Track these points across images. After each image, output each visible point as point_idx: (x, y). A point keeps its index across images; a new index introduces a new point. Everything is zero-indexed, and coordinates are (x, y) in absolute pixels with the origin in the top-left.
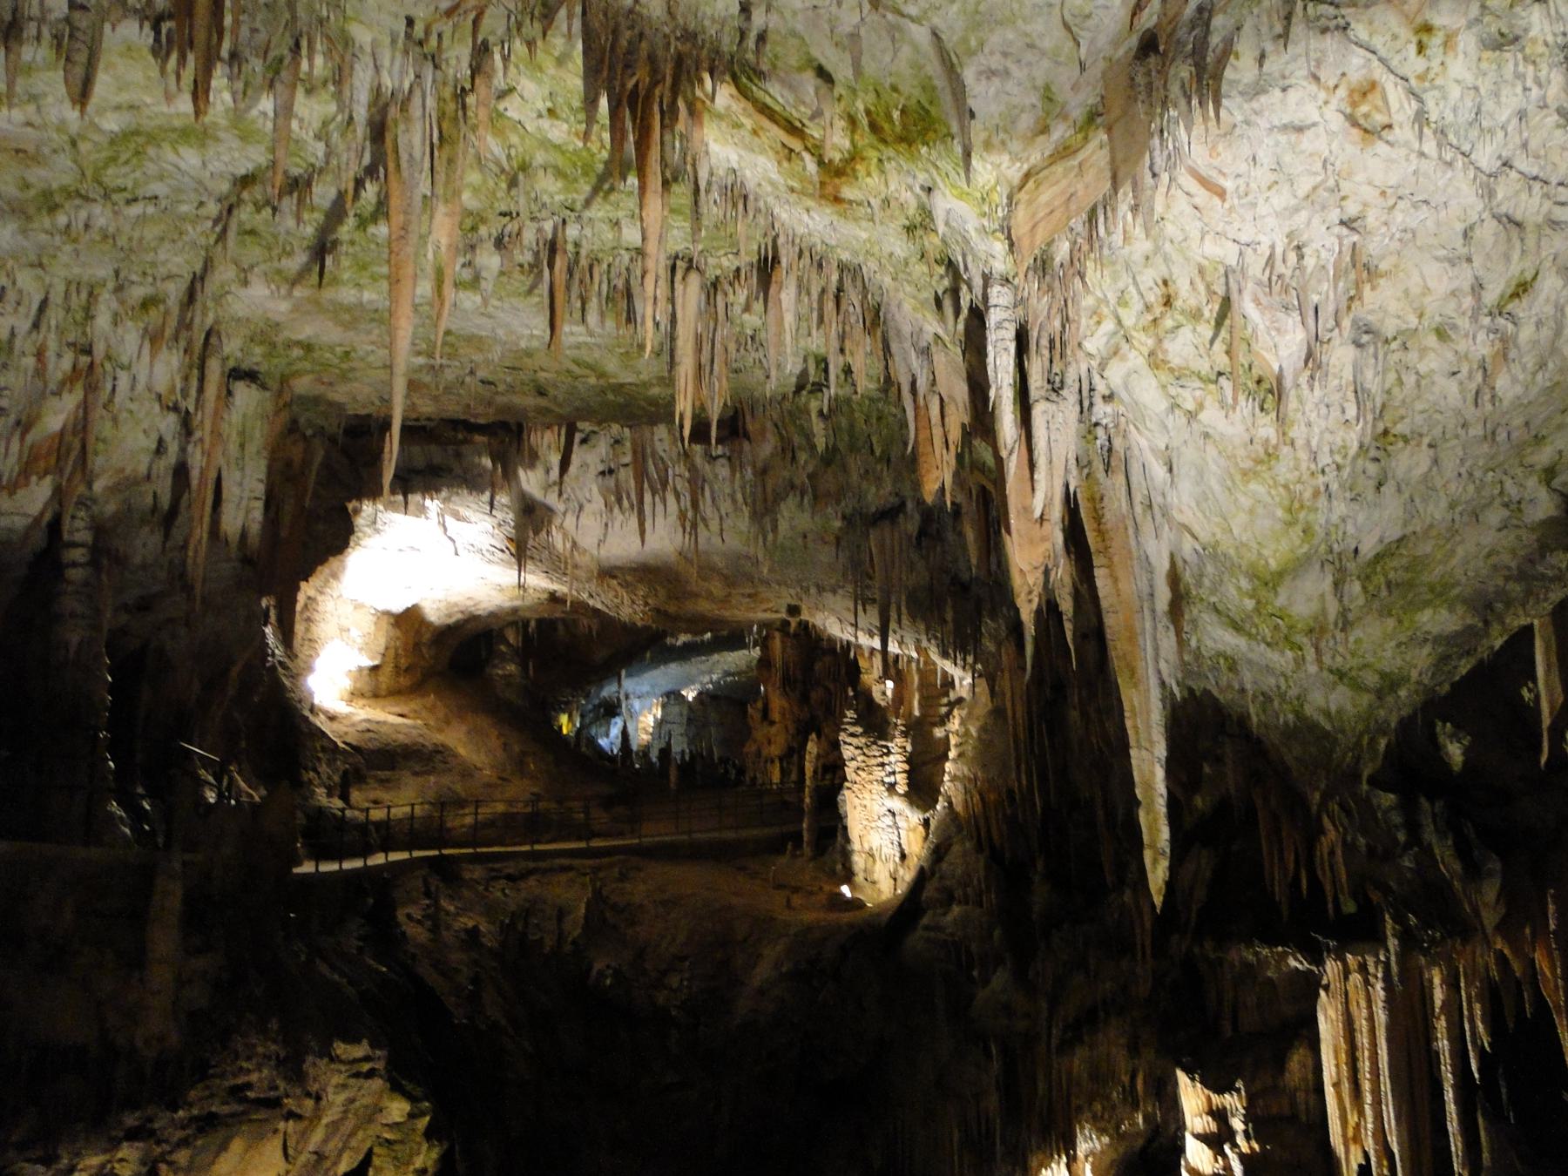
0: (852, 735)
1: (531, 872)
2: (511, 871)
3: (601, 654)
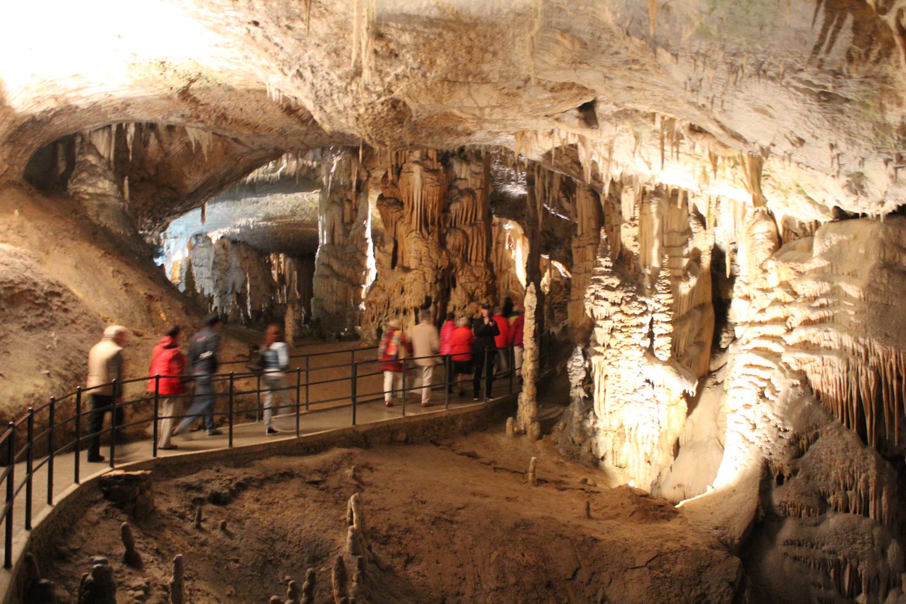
0: (608, 288)
1: (242, 487)
2: (215, 486)
3: (194, 180)
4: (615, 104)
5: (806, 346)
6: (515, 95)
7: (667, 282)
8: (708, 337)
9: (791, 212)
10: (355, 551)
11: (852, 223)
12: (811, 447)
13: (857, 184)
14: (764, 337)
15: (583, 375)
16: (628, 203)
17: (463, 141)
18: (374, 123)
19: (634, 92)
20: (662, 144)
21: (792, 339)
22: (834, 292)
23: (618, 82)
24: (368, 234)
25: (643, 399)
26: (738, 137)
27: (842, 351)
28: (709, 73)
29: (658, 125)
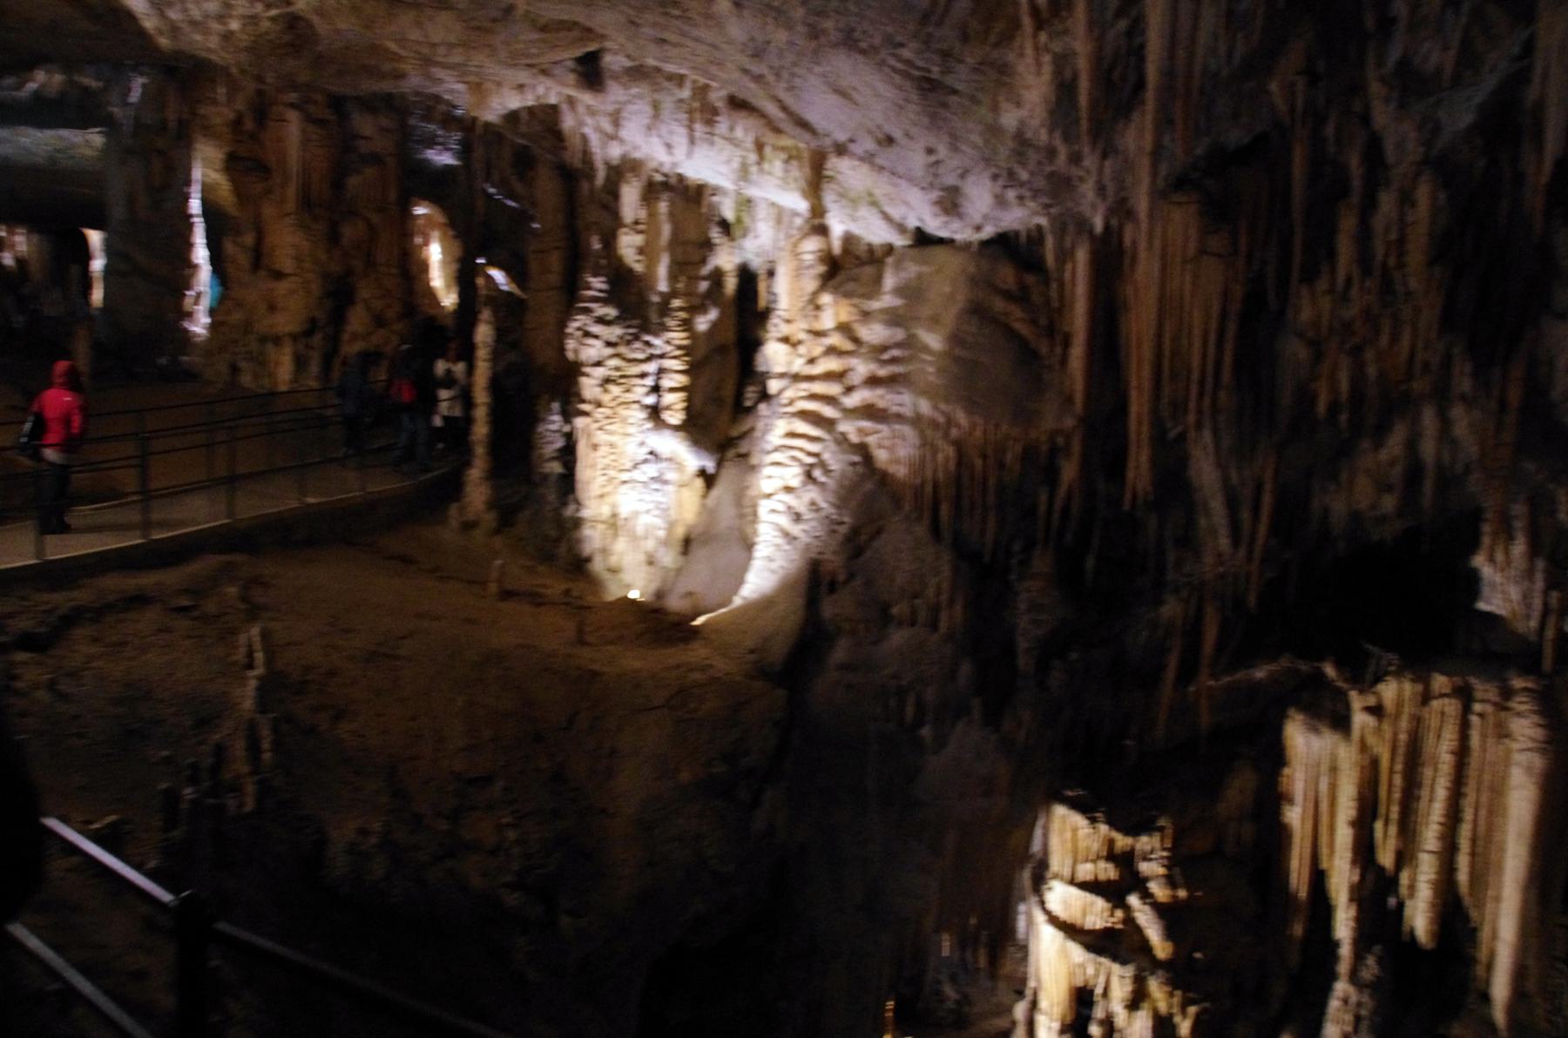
0: (601, 321)
2: (24, 624)
4: (628, 56)
5: (869, 412)
6: (487, 31)
7: (683, 315)
8: (729, 391)
9: (857, 229)
10: (263, 705)
11: (940, 253)
12: (876, 544)
13: (950, 203)
14: (813, 397)
15: (560, 443)
16: (630, 198)
17: (386, 86)
18: (252, 49)
19: (666, 47)
20: (692, 121)
21: (852, 401)
22: (909, 343)
23: (647, 30)
24: (195, 205)
25: (644, 478)
26: (804, 125)
27: (917, 421)
28: (781, 36)
29: (686, 93)
